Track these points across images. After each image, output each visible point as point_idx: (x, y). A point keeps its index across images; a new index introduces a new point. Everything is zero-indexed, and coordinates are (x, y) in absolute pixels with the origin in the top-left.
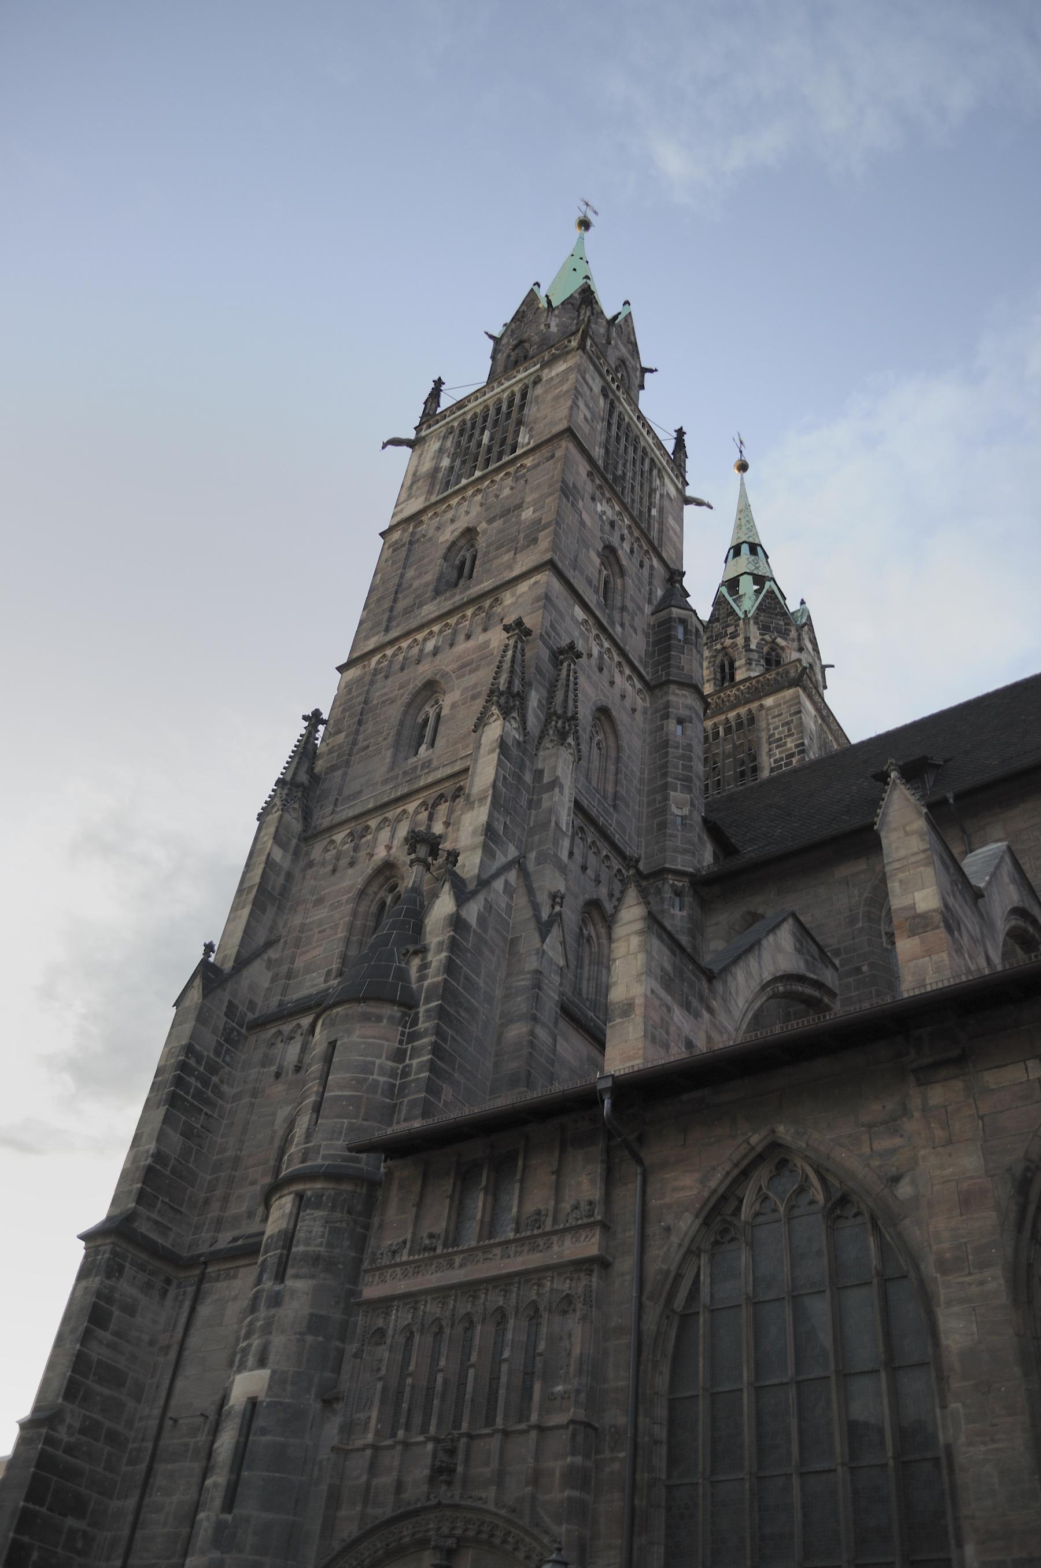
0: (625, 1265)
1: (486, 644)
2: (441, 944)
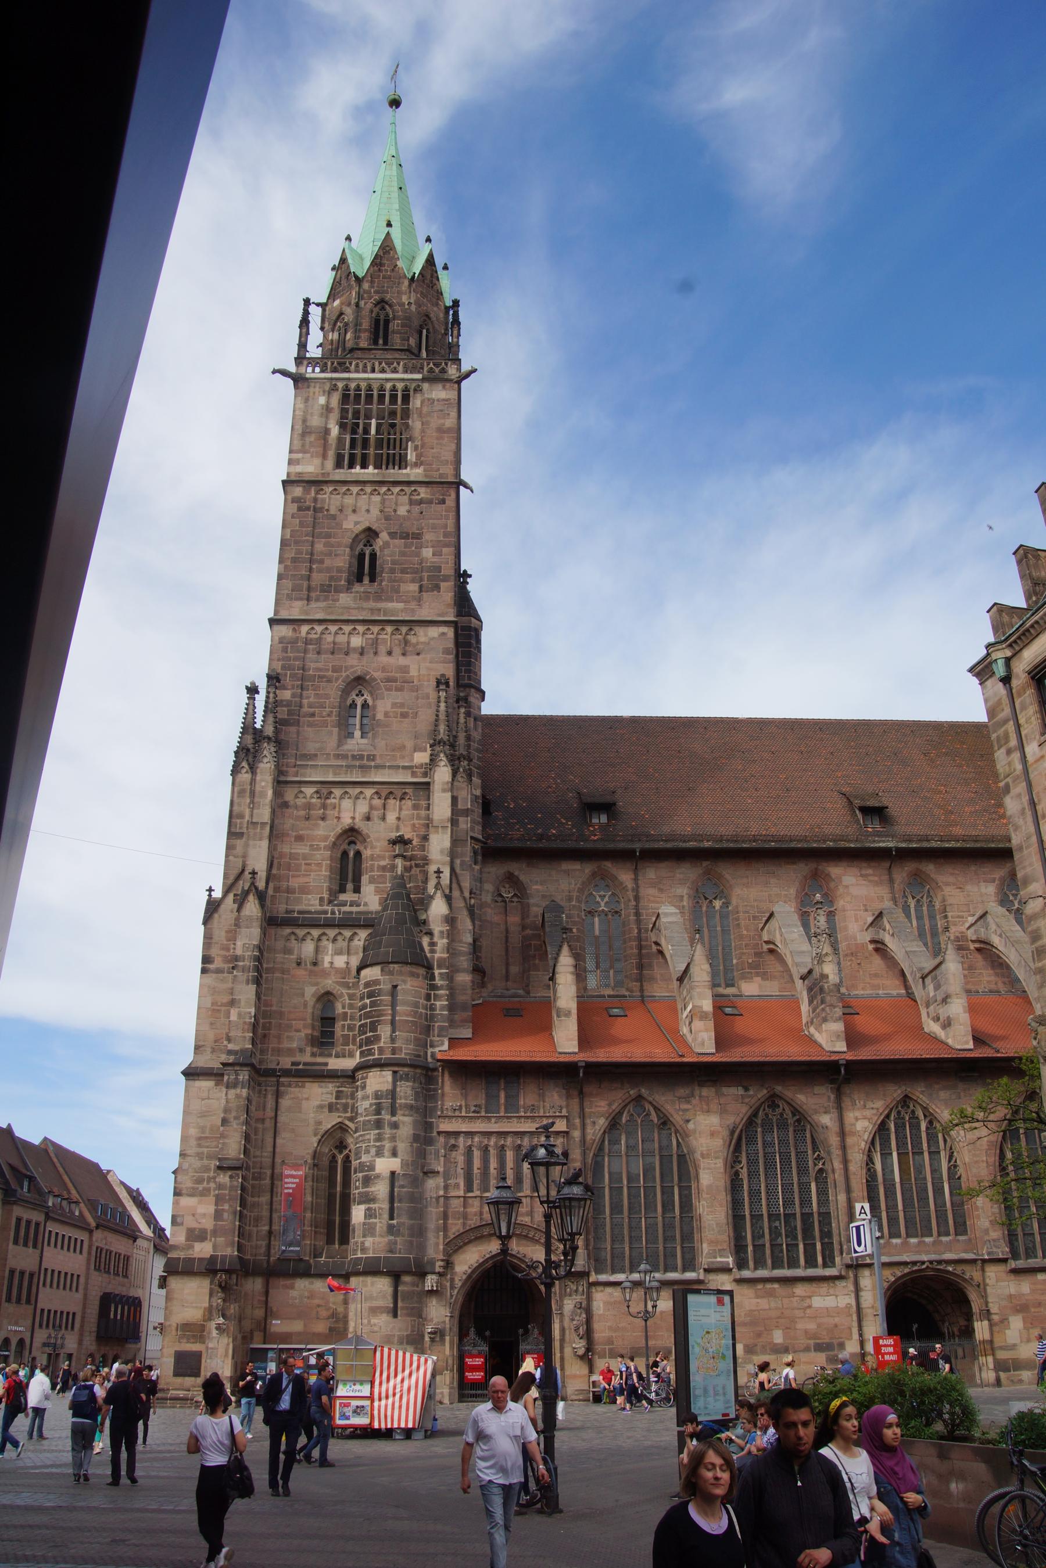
0: (576, 1134)
1: (405, 669)
2: (442, 932)
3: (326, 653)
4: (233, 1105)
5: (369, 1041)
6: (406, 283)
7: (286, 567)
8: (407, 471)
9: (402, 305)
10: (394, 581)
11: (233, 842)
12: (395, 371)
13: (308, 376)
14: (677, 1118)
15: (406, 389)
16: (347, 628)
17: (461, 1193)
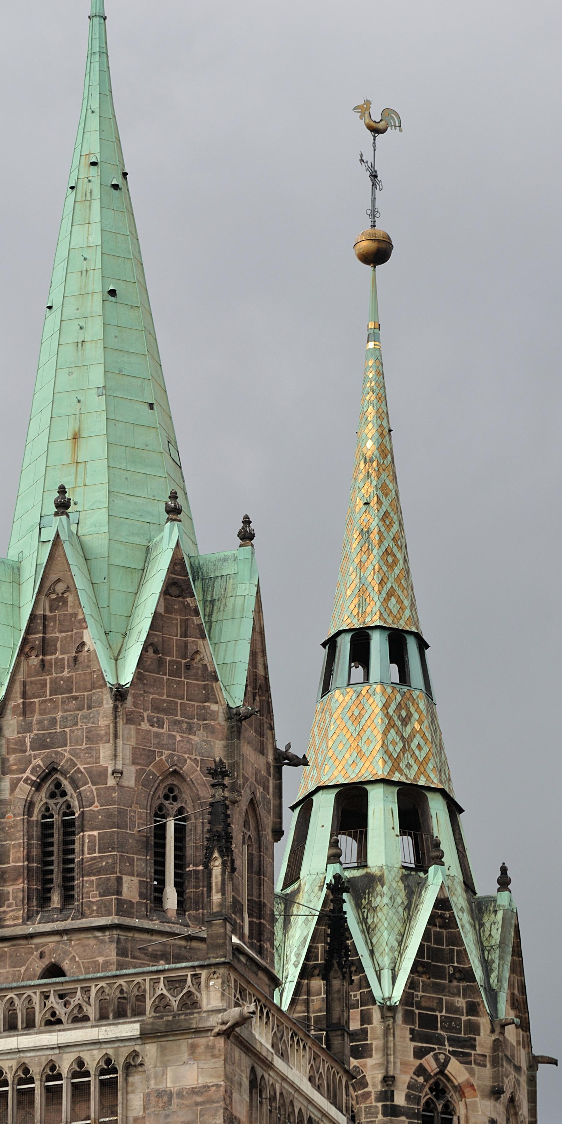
6: (108, 704)
9: (98, 777)
12: (80, 1019)
15: (108, 1066)
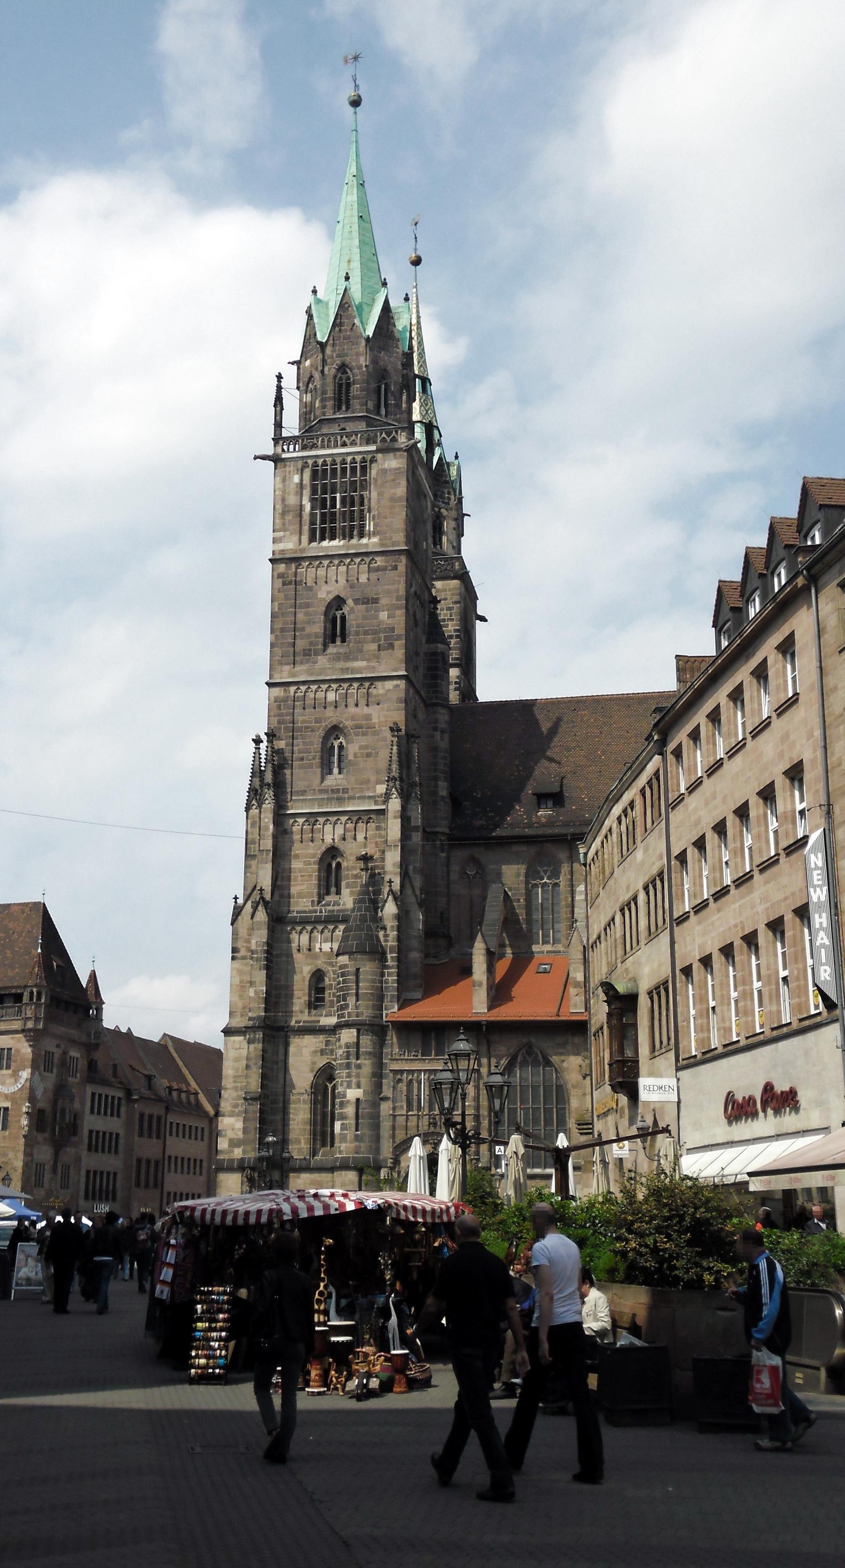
1: (368, 717)
2: (392, 927)
3: (309, 708)
4: (252, 1055)
5: (342, 1008)
6: (363, 343)
7: (276, 636)
8: (365, 541)
9: (360, 367)
10: (359, 642)
11: (250, 862)
12: (353, 444)
13: (284, 456)
14: (555, 1059)
15: (364, 460)
16: (324, 687)
17: (404, 1112)
